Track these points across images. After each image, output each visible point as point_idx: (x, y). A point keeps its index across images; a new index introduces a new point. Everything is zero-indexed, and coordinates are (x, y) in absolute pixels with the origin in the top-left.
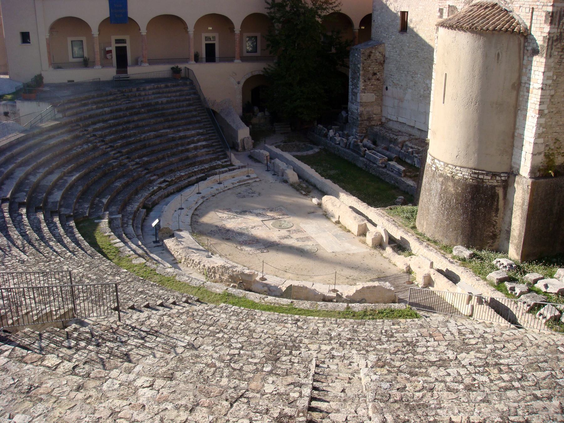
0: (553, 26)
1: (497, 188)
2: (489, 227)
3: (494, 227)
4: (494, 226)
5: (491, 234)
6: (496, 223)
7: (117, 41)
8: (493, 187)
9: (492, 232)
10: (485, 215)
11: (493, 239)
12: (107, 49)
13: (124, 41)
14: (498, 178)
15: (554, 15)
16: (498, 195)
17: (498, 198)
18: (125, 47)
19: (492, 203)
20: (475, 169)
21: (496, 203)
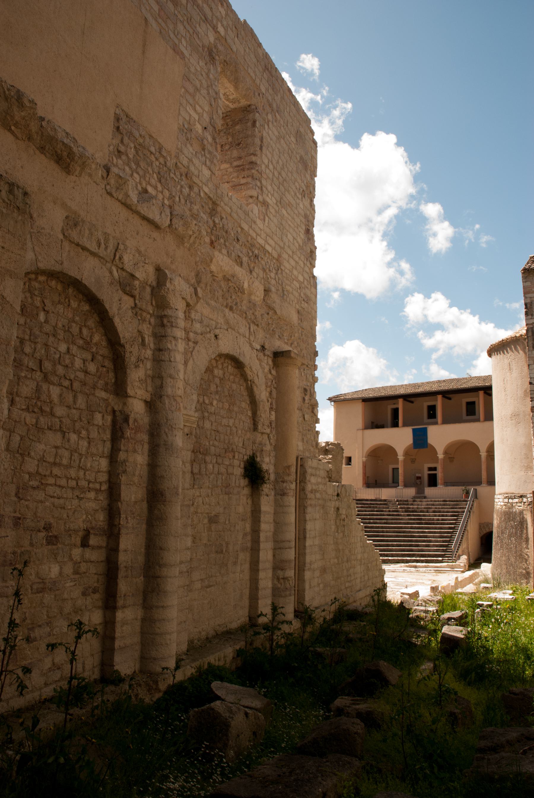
0: (530, 317)
1: (524, 512)
2: (521, 562)
3: (526, 562)
4: (526, 560)
5: (524, 571)
6: (529, 557)
7: (430, 469)
8: (521, 512)
9: (525, 569)
10: (516, 547)
11: (526, 579)
12: (417, 475)
13: (435, 469)
14: (525, 500)
15: (528, 306)
16: (526, 520)
17: (527, 524)
18: (435, 475)
19: (522, 531)
20: (507, 494)
21: (525, 531)
